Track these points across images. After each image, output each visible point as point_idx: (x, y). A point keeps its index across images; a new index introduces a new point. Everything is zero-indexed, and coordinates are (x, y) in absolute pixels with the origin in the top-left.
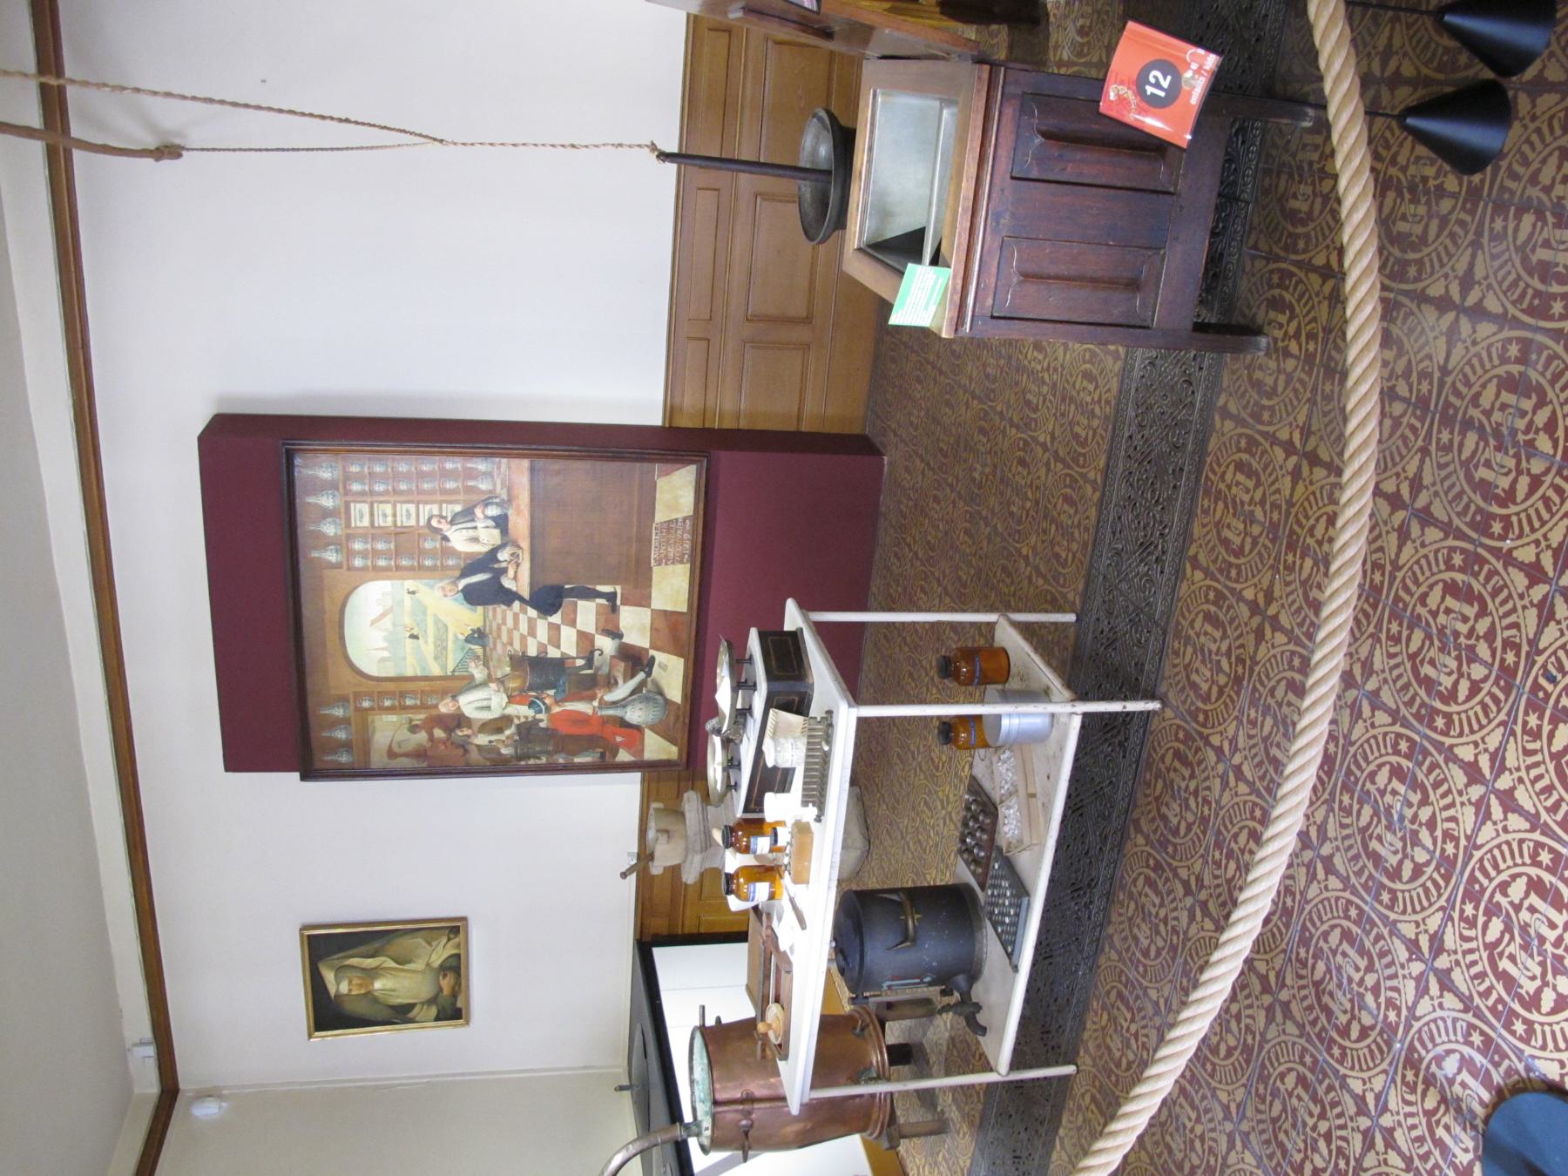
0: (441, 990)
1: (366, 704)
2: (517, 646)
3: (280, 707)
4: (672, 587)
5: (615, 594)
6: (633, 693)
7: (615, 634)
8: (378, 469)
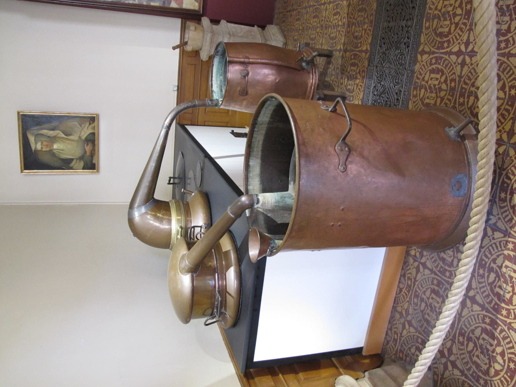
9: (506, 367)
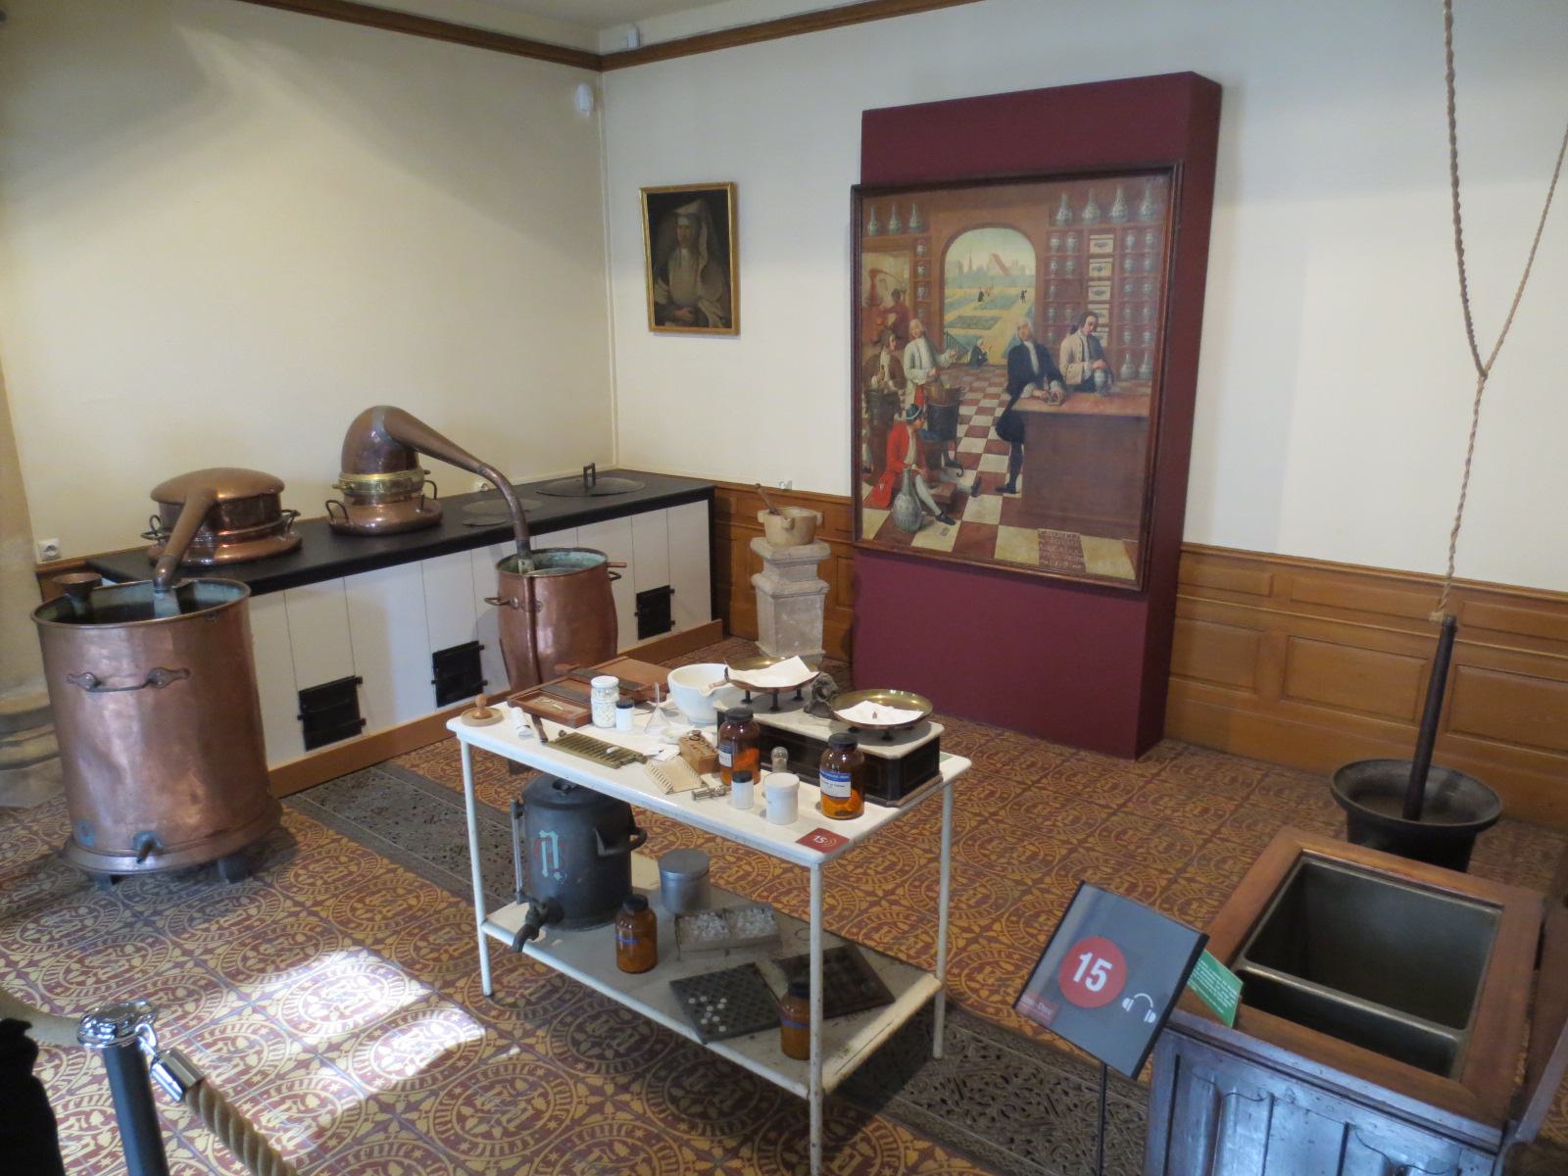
0: (680, 308)
1: (920, 249)
3: (919, 165)
4: (1018, 547)
5: (1013, 491)
6: (923, 503)
7: (977, 490)
9: (466, 1136)
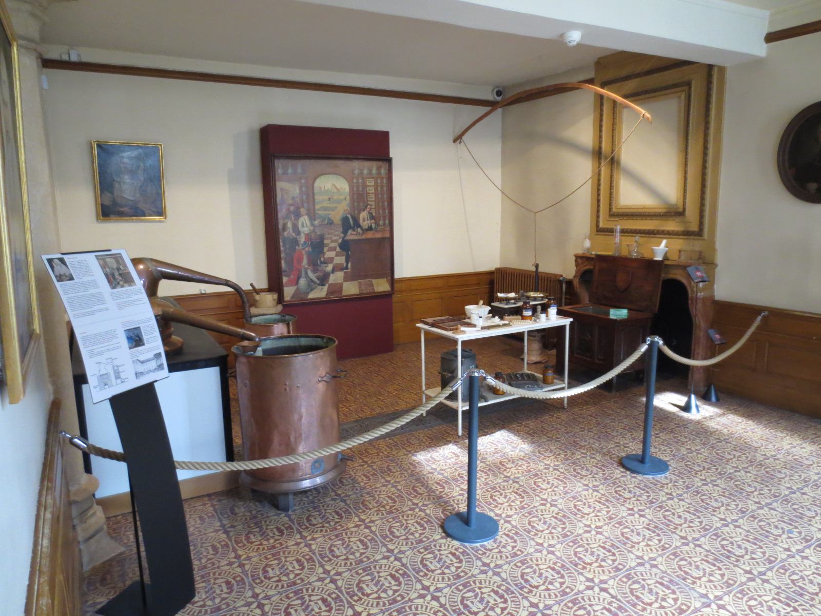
2: (327, 236)
3: (280, 146)
4: (351, 289)
6: (311, 280)
7: (333, 271)
8: (385, 188)
